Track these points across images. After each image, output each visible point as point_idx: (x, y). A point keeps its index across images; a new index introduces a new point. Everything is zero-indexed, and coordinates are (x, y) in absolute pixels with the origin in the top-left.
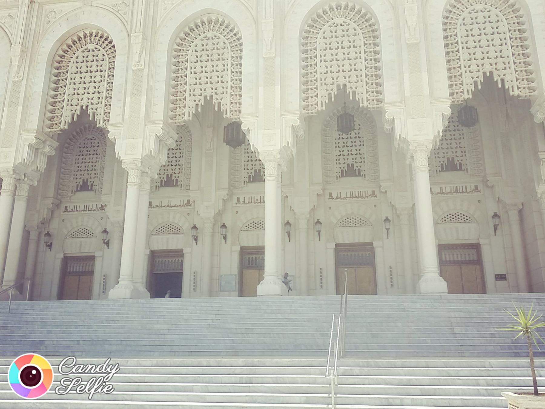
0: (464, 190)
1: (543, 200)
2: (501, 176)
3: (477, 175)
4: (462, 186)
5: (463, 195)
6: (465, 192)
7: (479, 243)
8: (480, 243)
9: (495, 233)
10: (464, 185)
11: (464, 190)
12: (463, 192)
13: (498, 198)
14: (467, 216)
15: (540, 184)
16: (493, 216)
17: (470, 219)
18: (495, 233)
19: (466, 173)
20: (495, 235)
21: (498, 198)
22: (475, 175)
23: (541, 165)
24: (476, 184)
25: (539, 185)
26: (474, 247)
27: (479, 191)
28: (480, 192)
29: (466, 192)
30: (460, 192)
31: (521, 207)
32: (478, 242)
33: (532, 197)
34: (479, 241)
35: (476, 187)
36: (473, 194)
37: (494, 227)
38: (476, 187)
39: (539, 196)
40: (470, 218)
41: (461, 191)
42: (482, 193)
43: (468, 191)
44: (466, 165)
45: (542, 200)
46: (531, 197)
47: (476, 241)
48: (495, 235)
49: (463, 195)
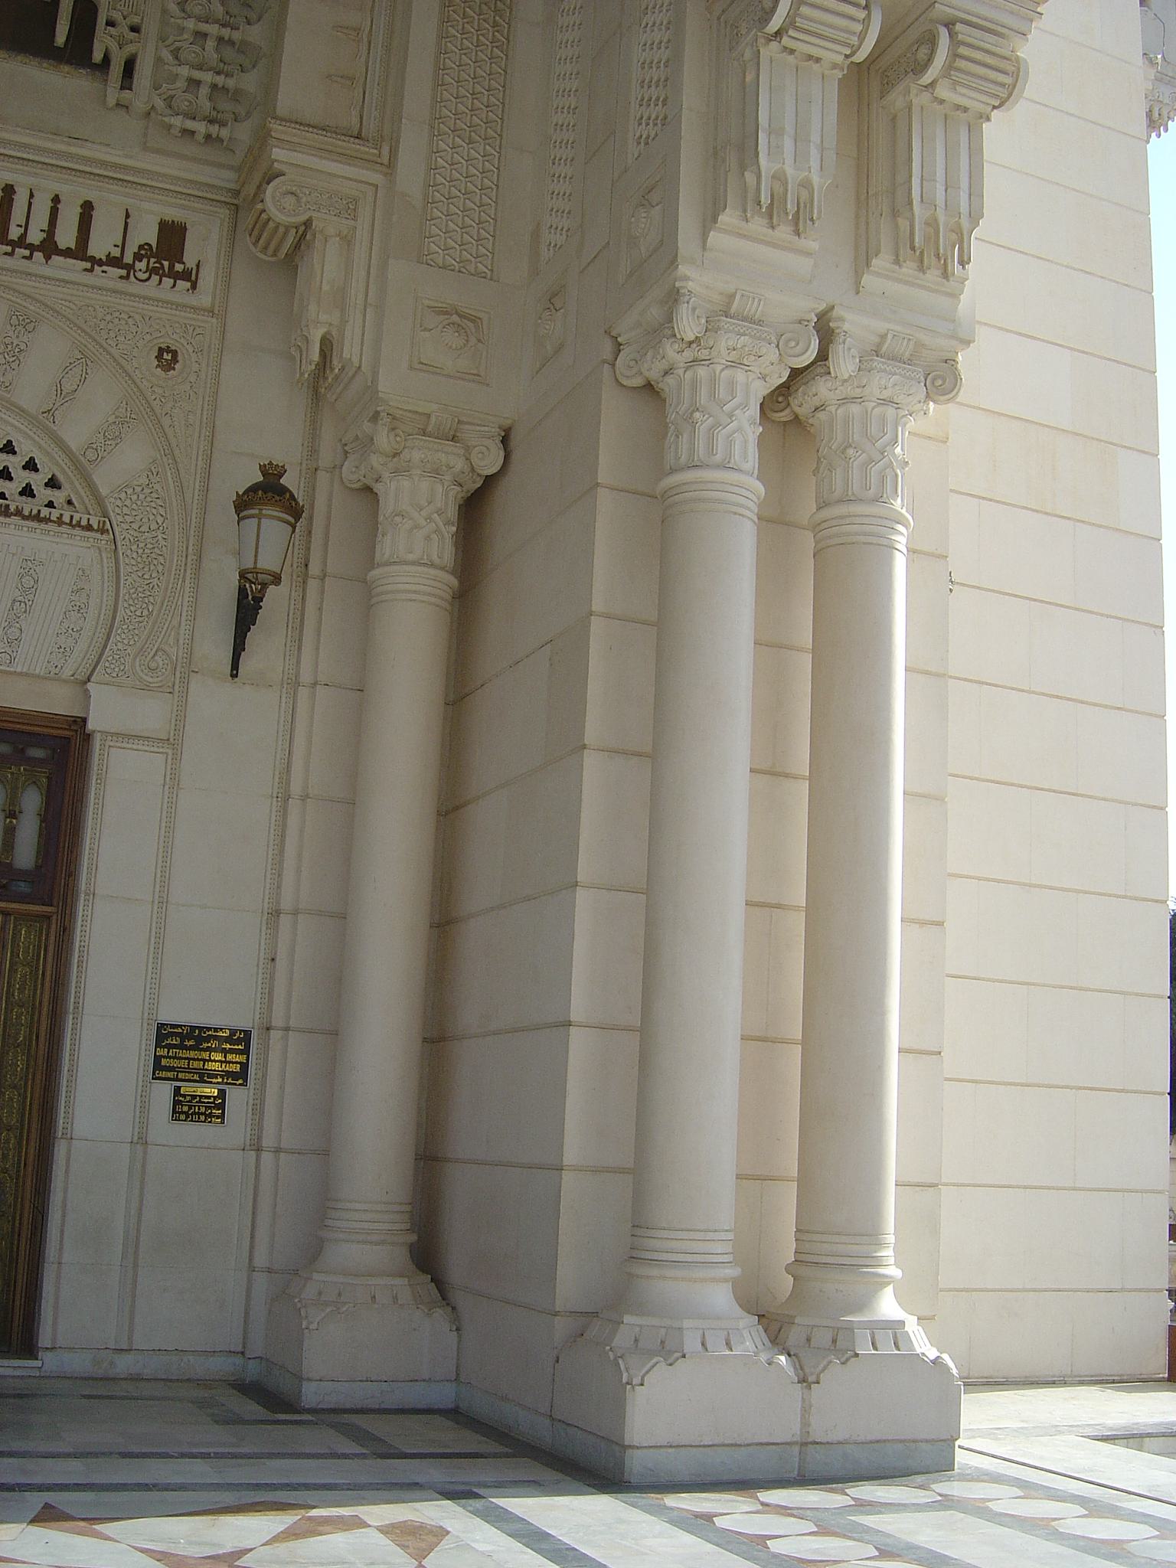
0: (66, 238)
1: (713, 381)
2: (391, 166)
3: (201, 127)
4: (56, 200)
5: (47, 271)
6: (67, 253)
7: (84, 720)
8: (91, 726)
9: (239, 648)
10: (74, 194)
11: (66, 238)
12: (49, 247)
13: (327, 347)
14: (31, 466)
15: (727, 218)
16: (253, 489)
17: (58, 497)
18: (239, 648)
19: (113, 94)
20: (234, 676)
21: (327, 347)
22: (177, 122)
23: (775, 24)
24: (173, 214)
25: (709, 219)
26: (37, 753)
27: (186, 275)
28: (194, 287)
29: (79, 251)
30: (21, 242)
31: (490, 464)
32: (76, 712)
33: (618, 347)
34: (87, 695)
35: (172, 236)
36: (133, 287)
37: (242, 592)
38: (172, 236)
39: (688, 325)
40: (53, 483)
41: (35, 237)
42: (204, 297)
43: (99, 247)
44: (135, 29)
45: (702, 372)
46: (608, 347)
47: (57, 702)
48: (234, 676)
49: (47, 271)
